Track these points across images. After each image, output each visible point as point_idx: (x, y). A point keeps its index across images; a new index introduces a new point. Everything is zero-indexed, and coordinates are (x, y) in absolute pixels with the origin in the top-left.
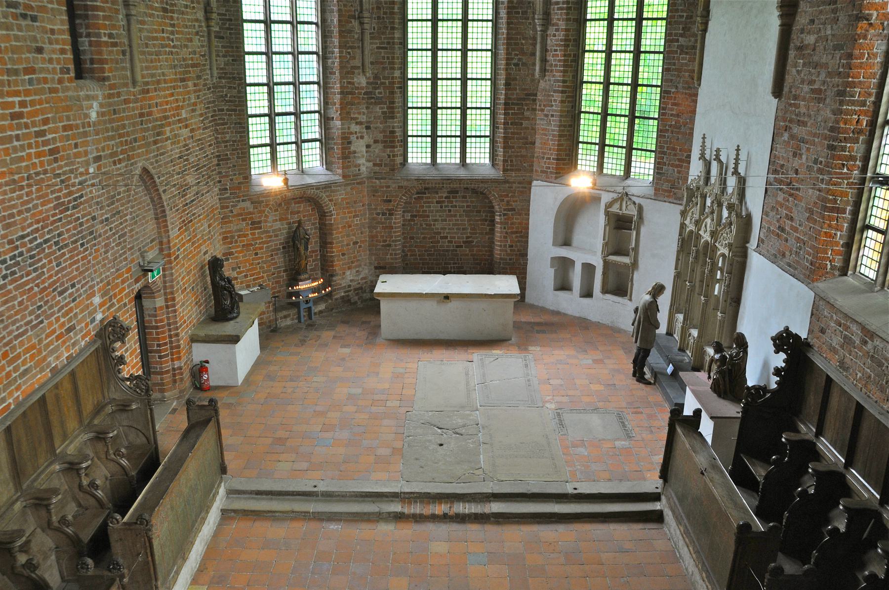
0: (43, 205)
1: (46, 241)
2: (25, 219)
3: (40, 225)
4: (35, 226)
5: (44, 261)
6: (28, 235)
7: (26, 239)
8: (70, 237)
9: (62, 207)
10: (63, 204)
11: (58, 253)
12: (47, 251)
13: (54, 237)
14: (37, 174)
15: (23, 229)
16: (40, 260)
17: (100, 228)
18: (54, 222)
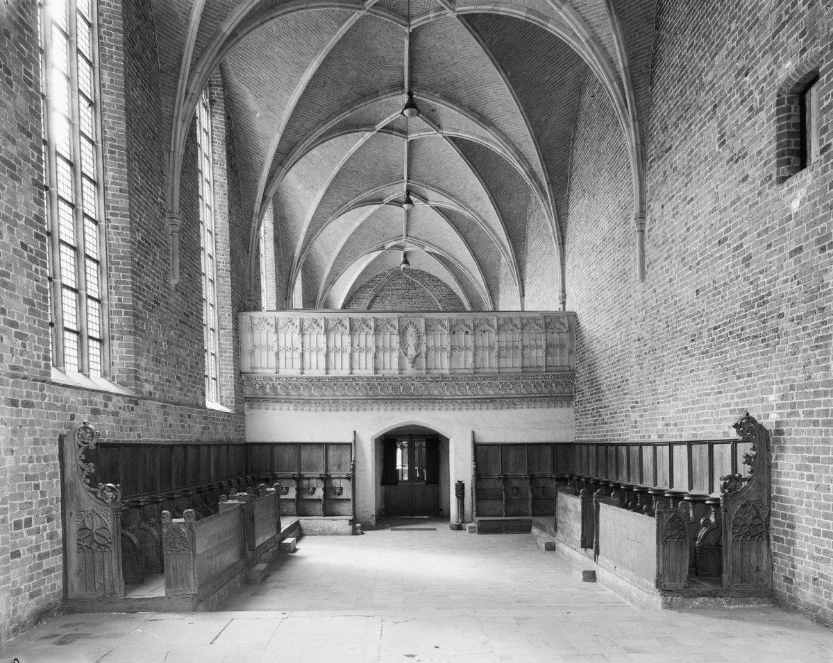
0: (732, 304)
1: (731, 333)
2: (719, 316)
3: (728, 320)
4: (725, 321)
5: (728, 348)
6: (719, 326)
7: (718, 330)
8: (751, 332)
9: (748, 305)
10: (748, 303)
11: (739, 344)
12: (731, 341)
13: (738, 330)
14: (731, 281)
15: (717, 321)
16: (724, 346)
17: (785, 325)
18: (740, 318)
